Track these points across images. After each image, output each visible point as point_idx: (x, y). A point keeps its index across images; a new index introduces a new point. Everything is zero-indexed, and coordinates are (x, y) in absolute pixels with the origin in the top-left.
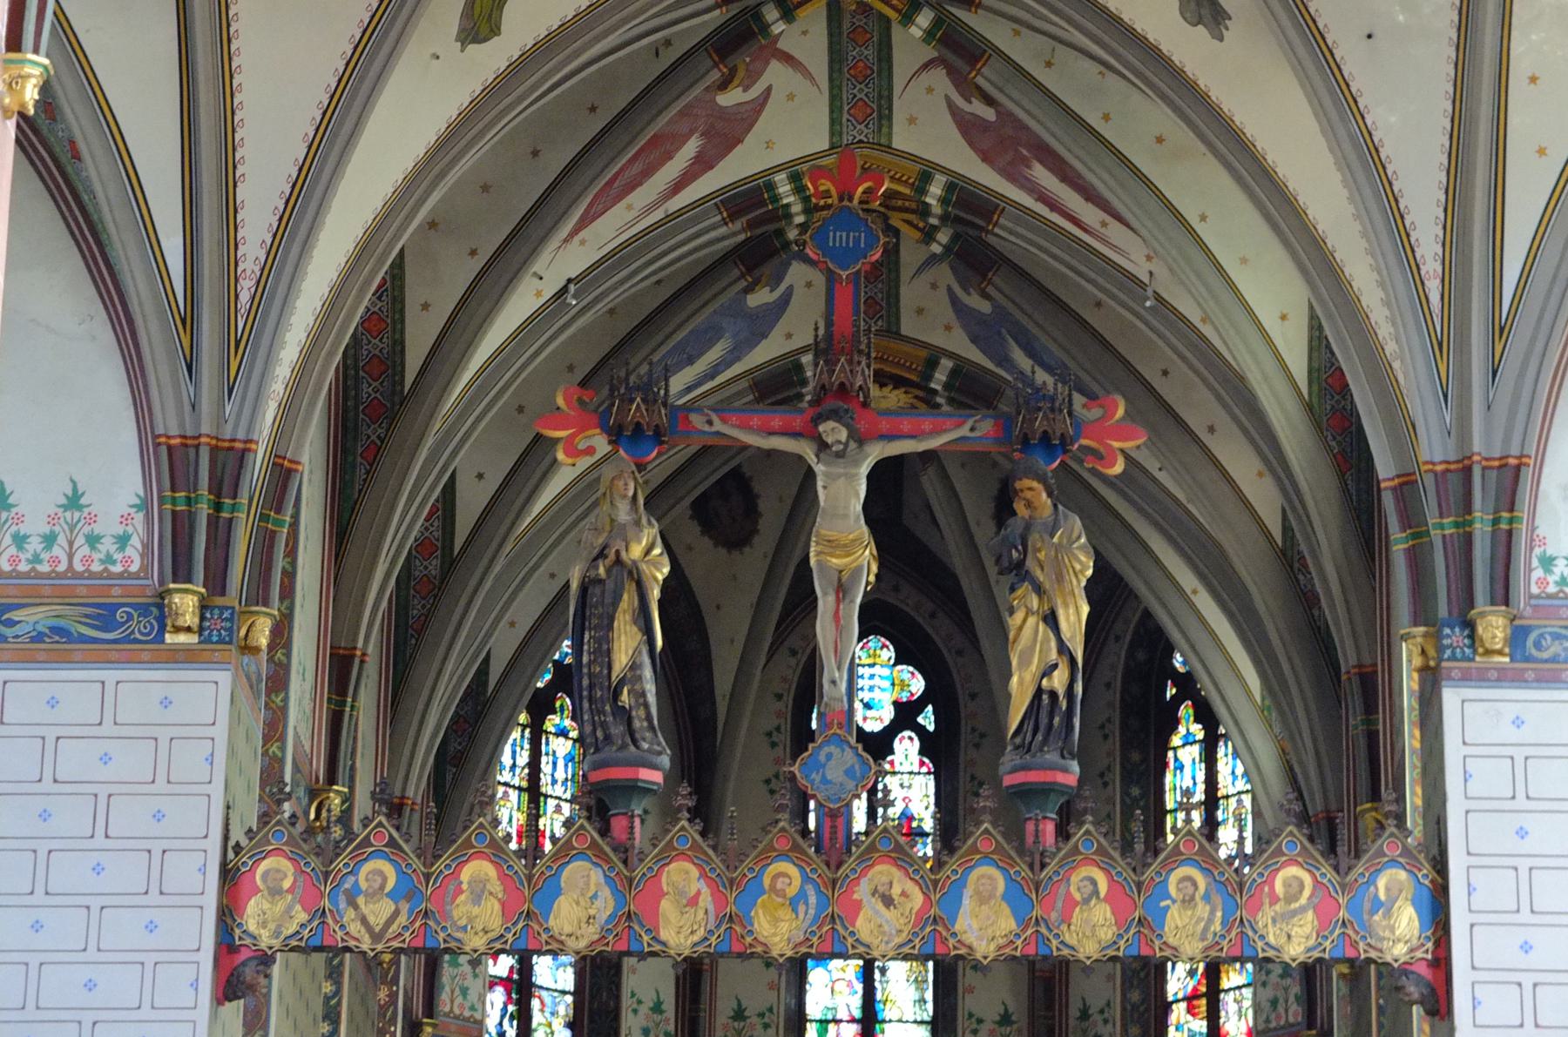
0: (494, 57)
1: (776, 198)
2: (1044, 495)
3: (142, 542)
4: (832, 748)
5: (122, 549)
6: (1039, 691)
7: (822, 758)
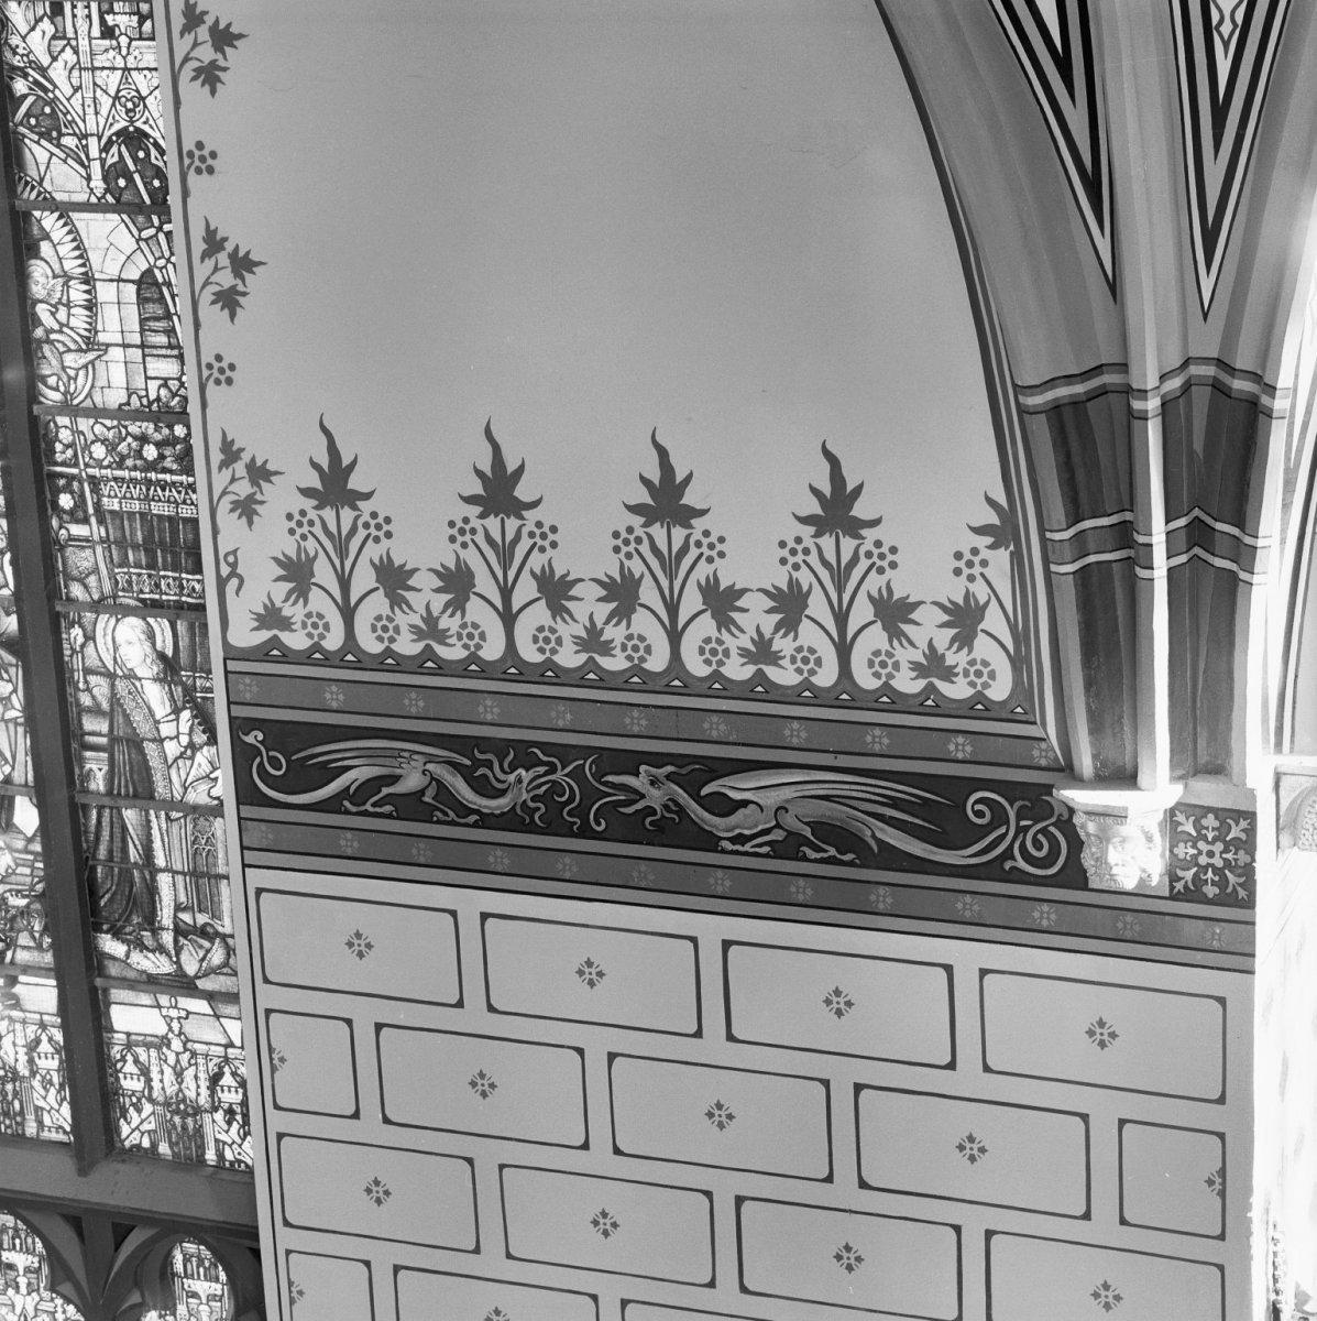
3: (1013, 627)
5: (965, 640)
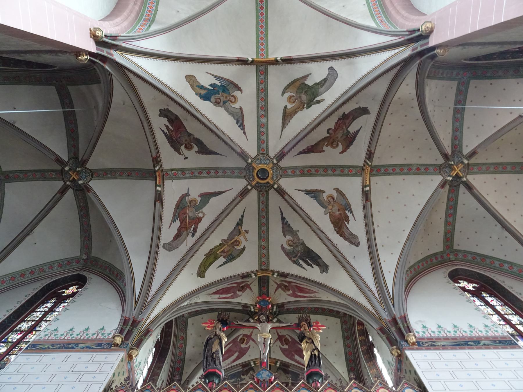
0: (203, 282)
1: (251, 365)
2: (307, 328)
4: (263, 371)
6: (312, 355)
7: (261, 373)
